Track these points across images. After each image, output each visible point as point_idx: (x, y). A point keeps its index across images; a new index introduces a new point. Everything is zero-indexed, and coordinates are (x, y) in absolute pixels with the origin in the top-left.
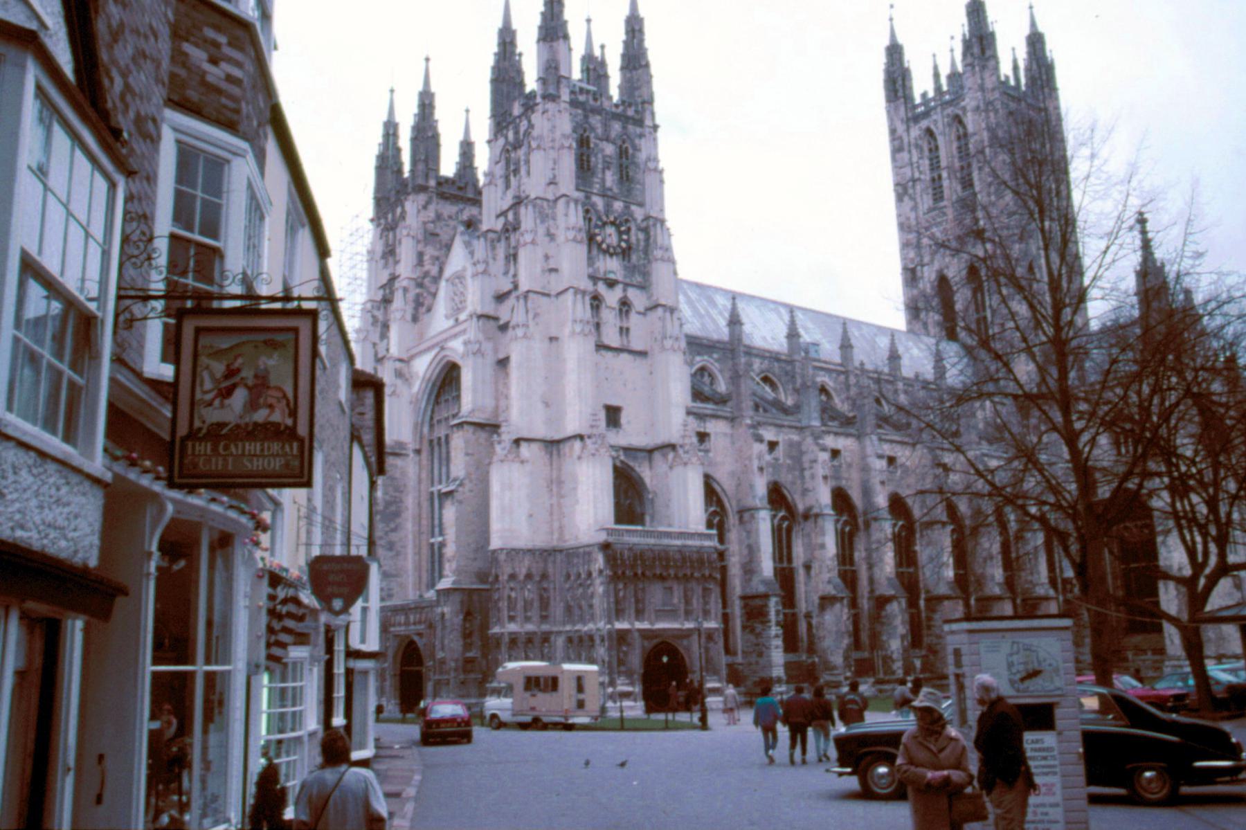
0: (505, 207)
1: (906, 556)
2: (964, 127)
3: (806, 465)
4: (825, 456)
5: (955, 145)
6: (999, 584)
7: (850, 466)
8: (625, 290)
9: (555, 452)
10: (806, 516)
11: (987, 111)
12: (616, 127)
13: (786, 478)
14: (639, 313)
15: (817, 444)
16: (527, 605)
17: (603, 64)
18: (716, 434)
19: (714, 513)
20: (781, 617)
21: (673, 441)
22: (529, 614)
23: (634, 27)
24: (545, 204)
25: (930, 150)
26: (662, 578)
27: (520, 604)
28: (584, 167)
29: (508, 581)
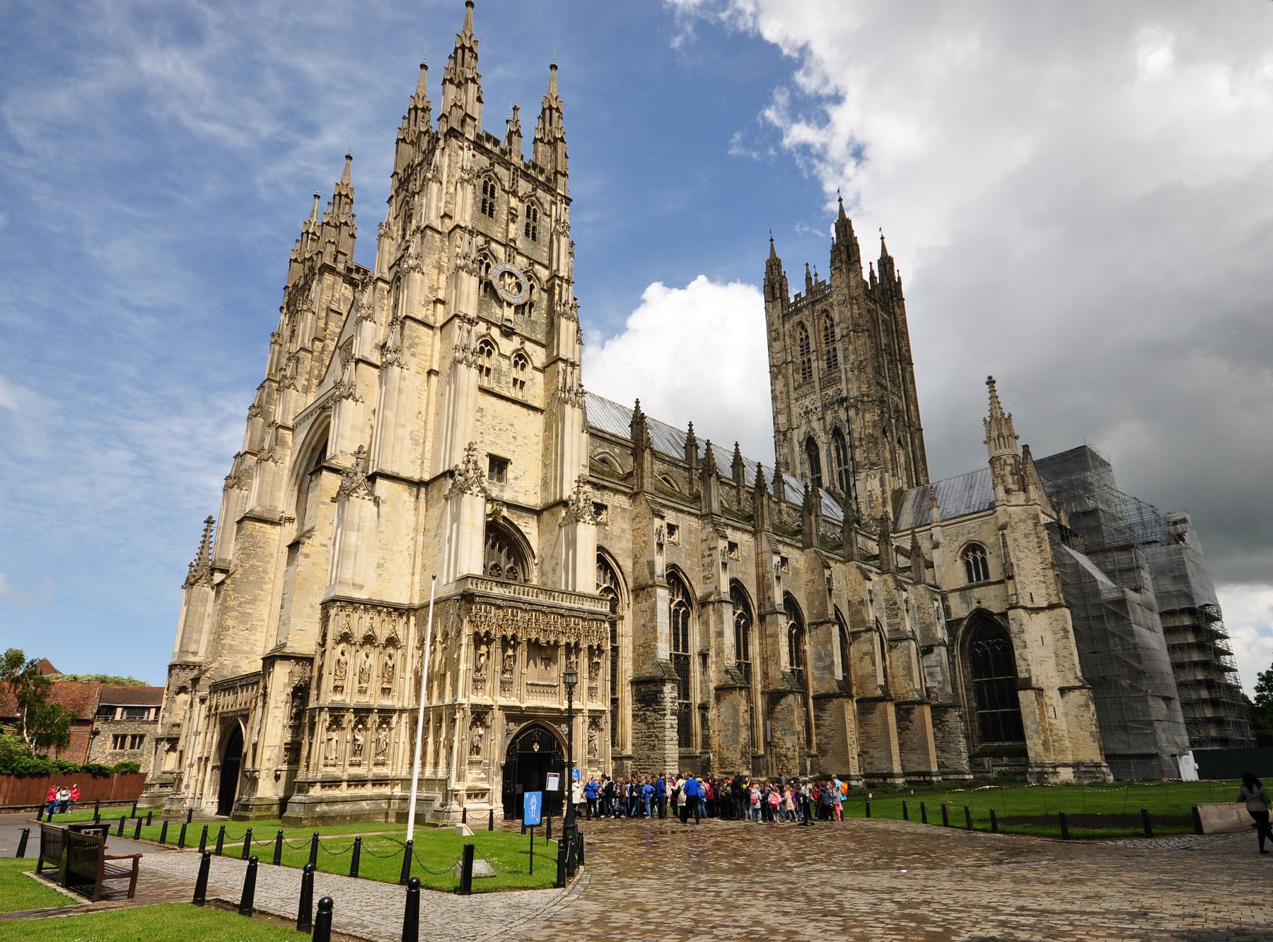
1: (797, 655)
2: (831, 320)
4: (722, 544)
5: (823, 333)
6: (881, 687)
7: (746, 560)
8: (522, 343)
9: (422, 495)
10: (704, 603)
11: (852, 304)
13: (684, 564)
16: (363, 674)
19: (607, 590)
21: (565, 497)
22: (364, 685)
25: (802, 339)
29: (338, 643)
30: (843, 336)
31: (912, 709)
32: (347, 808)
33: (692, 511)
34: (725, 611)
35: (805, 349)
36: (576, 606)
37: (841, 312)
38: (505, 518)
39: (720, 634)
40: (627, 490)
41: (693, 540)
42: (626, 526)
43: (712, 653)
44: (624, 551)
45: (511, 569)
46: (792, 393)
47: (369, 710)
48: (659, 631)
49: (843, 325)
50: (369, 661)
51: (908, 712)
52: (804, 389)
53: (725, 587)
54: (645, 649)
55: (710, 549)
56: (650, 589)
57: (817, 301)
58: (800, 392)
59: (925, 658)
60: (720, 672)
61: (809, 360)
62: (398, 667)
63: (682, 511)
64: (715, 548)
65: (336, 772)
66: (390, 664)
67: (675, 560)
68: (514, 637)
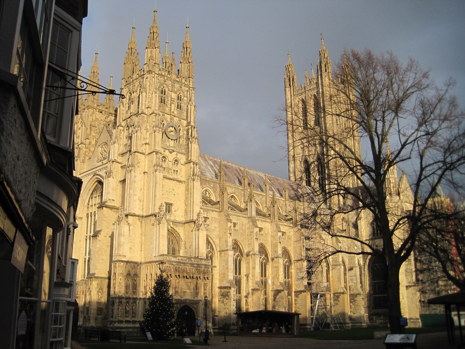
9: (143, 222)
10: (248, 255)
13: (240, 239)
18: (212, 218)
28: (162, 101)
31: (340, 296)
32: (126, 330)
38: (171, 227)
39: (254, 268)
47: (129, 298)
50: (129, 282)
51: (338, 297)
53: (257, 249)
54: (223, 275)
56: (226, 252)
59: (350, 271)
65: (122, 319)
66: (135, 283)
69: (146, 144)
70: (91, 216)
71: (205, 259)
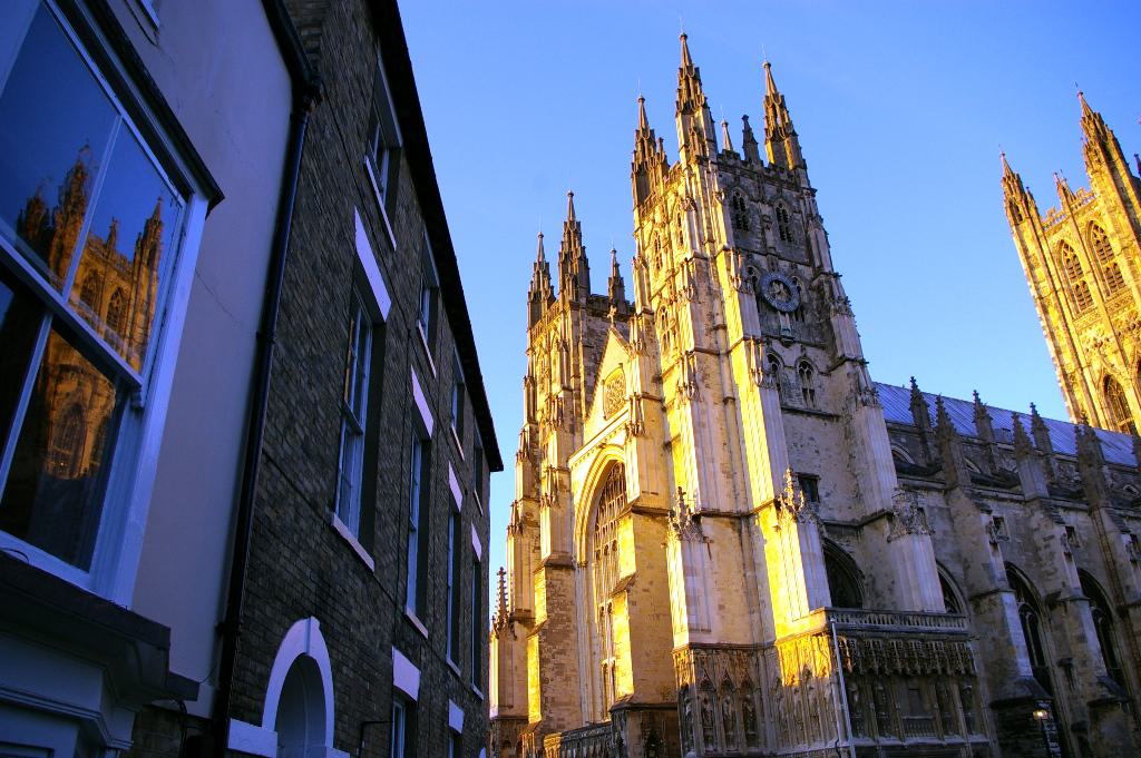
0: (659, 287)
2: (1102, 231)
3: (1041, 543)
4: (1060, 531)
7: (1088, 545)
12: (770, 190)
13: (1020, 561)
14: (822, 373)
15: (1051, 516)
16: (728, 723)
17: (748, 132)
18: (931, 508)
20: (1054, 728)
22: (731, 733)
23: (777, 103)
24: (703, 262)
25: (1068, 260)
26: (905, 676)
27: (718, 723)
30: (1124, 248)
33: (1015, 497)
34: (1081, 610)
35: (1076, 270)
36: (933, 628)
37: (1114, 221)
38: (825, 539)
39: (1082, 639)
40: (940, 486)
41: (1023, 531)
42: (948, 527)
43: (1075, 662)
44: (952, 556)
45: (841, 592)
46: (1071, 326)
48: (1014, 643)
49: (1121, 235)
52: (1086, 318)
53: (1075, 582)
55: (1045, 539)
56: (993, 597)
57: (1077, 213)
58: (1080, 323)
60: (1091, 684)
61: (1084, 283)
62: (758, 713)
63: (1003, 500)
64: (1052, 537)
66: (750, 709)
67: (1008, 558)
68: (881, 670)
69: (717, 328)
70: (606, 554)
71: (947, 617)
